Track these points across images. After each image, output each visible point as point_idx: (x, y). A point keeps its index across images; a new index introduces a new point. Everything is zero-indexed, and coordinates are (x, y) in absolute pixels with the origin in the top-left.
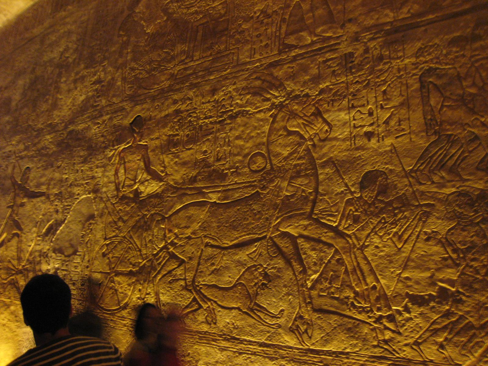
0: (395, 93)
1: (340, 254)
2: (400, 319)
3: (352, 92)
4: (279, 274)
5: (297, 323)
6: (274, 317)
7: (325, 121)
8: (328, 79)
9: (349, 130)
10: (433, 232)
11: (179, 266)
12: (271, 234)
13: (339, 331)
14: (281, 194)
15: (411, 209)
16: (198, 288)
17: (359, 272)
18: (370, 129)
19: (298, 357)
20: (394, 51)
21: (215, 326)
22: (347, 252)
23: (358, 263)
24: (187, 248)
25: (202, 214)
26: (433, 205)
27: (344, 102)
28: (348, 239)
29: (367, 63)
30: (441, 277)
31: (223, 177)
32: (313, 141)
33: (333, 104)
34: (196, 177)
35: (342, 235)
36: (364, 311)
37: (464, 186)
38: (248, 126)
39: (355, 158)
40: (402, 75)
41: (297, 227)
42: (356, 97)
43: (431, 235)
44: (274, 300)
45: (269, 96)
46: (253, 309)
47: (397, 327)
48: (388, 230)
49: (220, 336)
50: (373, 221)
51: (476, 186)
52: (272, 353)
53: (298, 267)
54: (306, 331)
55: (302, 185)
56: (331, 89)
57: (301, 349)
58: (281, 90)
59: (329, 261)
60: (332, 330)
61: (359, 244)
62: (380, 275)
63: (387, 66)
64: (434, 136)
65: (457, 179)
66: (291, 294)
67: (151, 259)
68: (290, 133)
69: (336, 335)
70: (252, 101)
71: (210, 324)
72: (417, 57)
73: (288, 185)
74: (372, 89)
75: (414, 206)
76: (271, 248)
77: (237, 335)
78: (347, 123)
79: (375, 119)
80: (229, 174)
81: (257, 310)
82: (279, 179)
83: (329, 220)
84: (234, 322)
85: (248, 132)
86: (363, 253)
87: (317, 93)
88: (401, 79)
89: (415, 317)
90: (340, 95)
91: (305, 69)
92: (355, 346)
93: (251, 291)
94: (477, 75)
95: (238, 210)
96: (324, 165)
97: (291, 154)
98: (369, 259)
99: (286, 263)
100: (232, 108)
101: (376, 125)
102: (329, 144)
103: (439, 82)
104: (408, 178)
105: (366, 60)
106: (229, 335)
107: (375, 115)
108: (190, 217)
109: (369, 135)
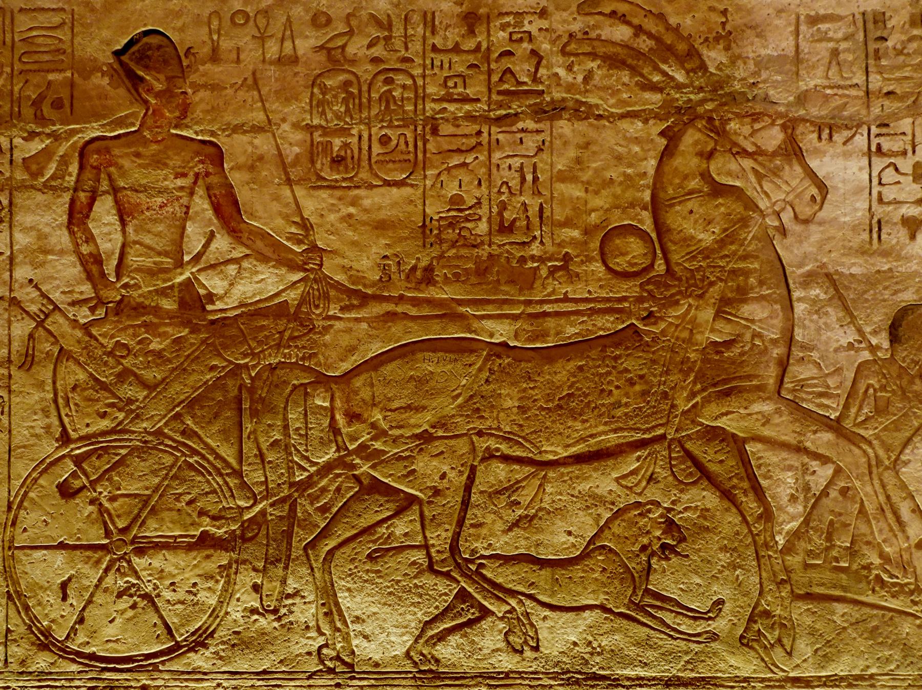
1: (849, 477)
5: (756, 627)
6: (697, 616)
11: (397, 513)
12: (677, 431)
13: (855, 635)
17: (889, 515)
23: (888, 497)
24: (420, 465)
25: (462, 376)
27: (858, 137)
28: (865, 447)
34: (429, 269)
36: (902, 591)
38: (594, 148)
39: (879, 272)
41: (743, 417)
42: (884, 130)
44: (698, 581)
45: (656, 78)
46: (643, 604)
53: (751, 505)
54: (779, 640)
55: (753, 321)
57: (769, 680)
59: (825, 493)
60: (838, 634)
66: (739, 567)
67: (290, 496)
68: (718, 190)
69: (847, 644)
70: (606, 82)
76: (681, 463)
83: (820, 406)
84: (591, 638)
85: (594, 165)
87: (791, 99)
92: (888, 660)
95: (581, 368)
96: (809, 280)
99: (721, 497)
100: (541, 88)
102: (815, 233)
106: (580, 673)
108: (420, 382)
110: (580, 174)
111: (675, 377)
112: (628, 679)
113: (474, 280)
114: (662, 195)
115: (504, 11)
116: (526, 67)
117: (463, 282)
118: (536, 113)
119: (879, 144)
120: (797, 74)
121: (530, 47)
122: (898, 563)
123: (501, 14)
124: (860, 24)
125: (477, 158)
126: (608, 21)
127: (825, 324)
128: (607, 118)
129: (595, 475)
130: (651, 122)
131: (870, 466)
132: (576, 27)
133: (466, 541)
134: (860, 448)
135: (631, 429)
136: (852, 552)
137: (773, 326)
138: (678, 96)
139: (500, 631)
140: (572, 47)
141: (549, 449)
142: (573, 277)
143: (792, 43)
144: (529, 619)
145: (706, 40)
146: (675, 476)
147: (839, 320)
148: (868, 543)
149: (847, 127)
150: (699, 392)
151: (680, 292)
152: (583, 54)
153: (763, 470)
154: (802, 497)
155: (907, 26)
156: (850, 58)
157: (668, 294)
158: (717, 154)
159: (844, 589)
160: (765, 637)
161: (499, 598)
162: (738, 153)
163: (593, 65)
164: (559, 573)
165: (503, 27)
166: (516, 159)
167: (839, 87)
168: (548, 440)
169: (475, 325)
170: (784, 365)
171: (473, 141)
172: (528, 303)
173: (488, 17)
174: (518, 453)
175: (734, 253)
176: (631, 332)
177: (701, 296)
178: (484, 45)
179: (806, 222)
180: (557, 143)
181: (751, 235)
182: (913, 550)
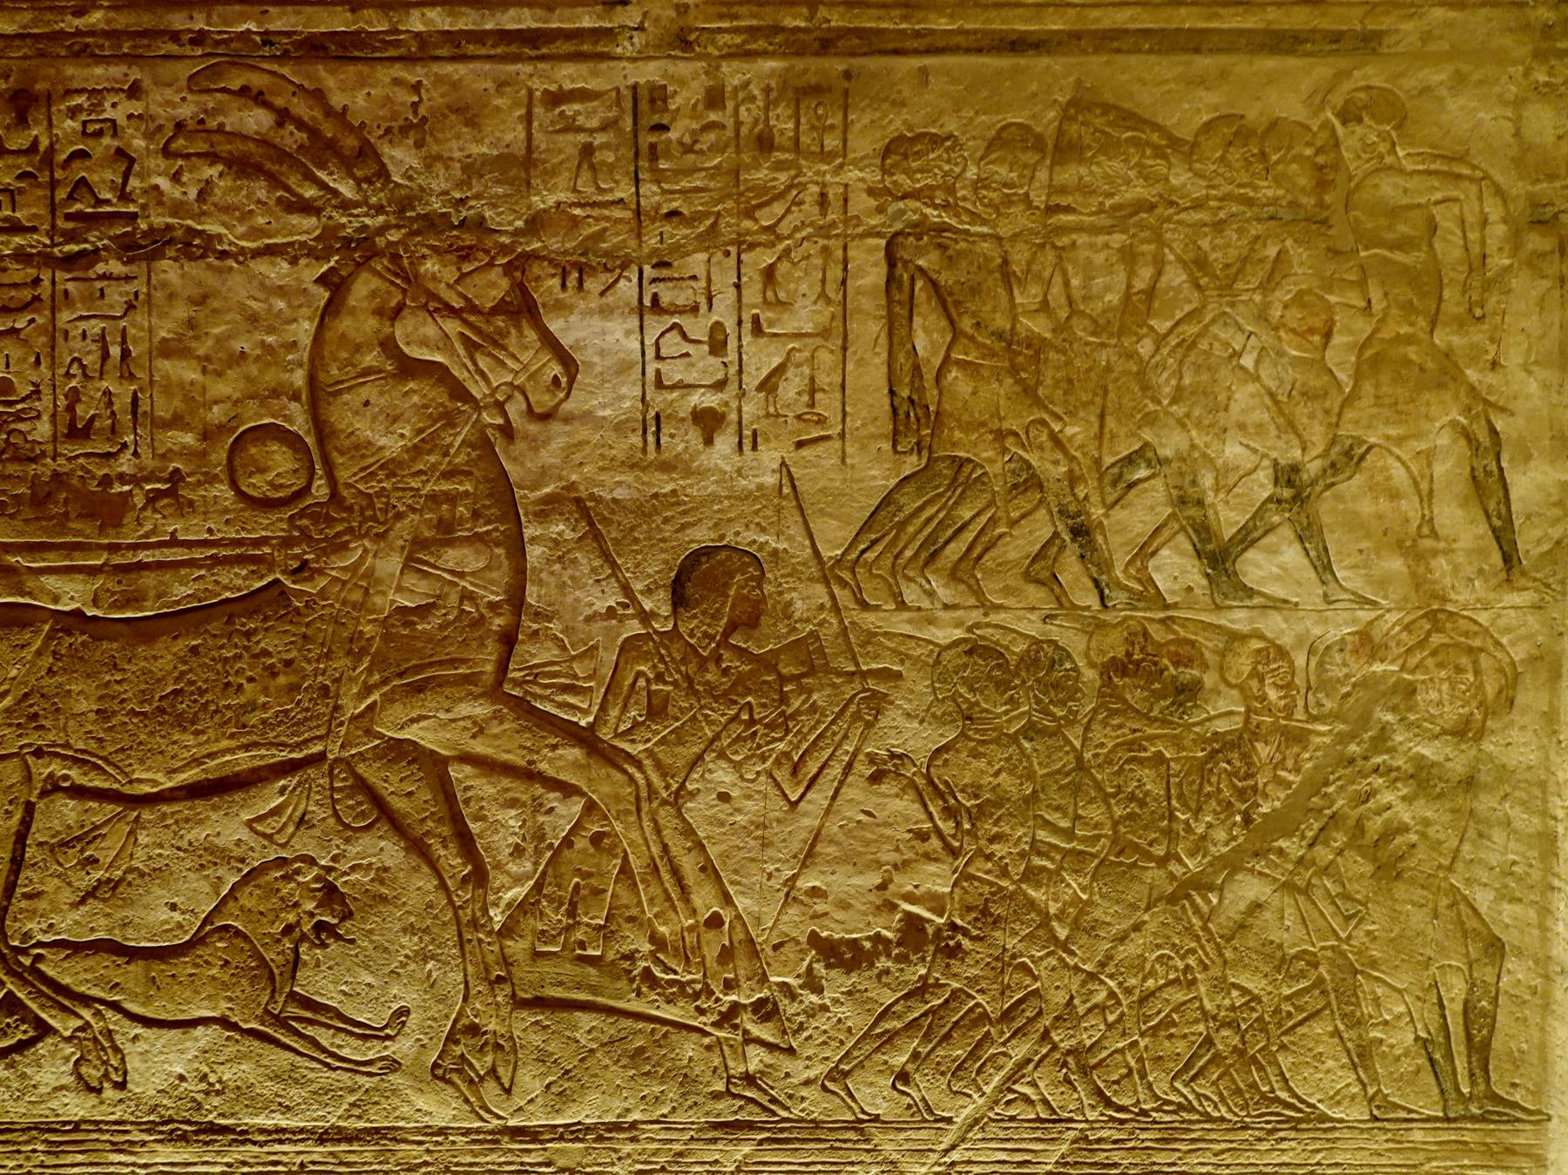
0: (804, 288)
1: (605, 817)
2: (791, 1011)
3: (654, 252)
4: (384, 891)
5: (458, 1050)
6: (368, 1034)
7: (550, 342)
8: (563, 179)
9: (638, 392)
10: (893, 756)
14: (378, 600)
15: (834, 685)
16: (27, 961)
17: (666, 876)
18: (711, 400)
19: (469, 1159)
20: (813, 128)
21: (119, 1095)
22: (627, 812)
23: (665, 848)
26: (899, 675)
27: (622, 283)
28: (631, 770)
29: (716, 148)
30: (909, 888)
31: (106, 510)
32: (505, 414)
33: (581, 281)
35: (610, 757)
37: (988, 625)
39: (656, 496)
40: (833, 224)
41: (444, 725)
42: (665, 273)
43: (890, 766)
45: (310, 192)
47: (784, 1032)
48: (759, 746)
49: (150, 1128)
50: (714, 716)
51: (1022, 627)
52: (369, 1157)
53: (453, 863)
54: (493, 1071)
55: (461, 575)
56: (575, 222)
57: (478, 1131)
58: (369, 181)
59: (567, 842)
61: (667, 787)
62: (732, 883)
63: (783, 177)
64: (914, 458)
65: (972, 601)
68: (409, 368)
71: (99, 1091)
72: (885, 171)
73: (406, 567)
74: (727, 254)
75: (839, 674)
77: (222, 1115)
78: (631, 366)
79: (733, 370)
80: (139, 501)
81: (300, 1019)
82: (366, 542)
83: (561, 705)
84: (206, 1069)
85: (216, 331)
86: (680, 815)
87: (519, 224)
88: (828, 237)
89: (836, 1001)
90: (606, 254)
91: (470, 114)
93: (269, 956)
94: (1058, 279)
95: (194, 650)
96: (547, 509)
97: (416, 451)
98: (701, 834)
99: (406, 849)
100: (132, 208)
101: (732, 388)
102: (559, 436)
103: (946, 278)
104: (828, 585)
105: (711, 136)
106: (188, 1122)
107: (732, 356)
109: (708, 422)
110: (193, 345)
111: (341, 663)
112: (262, 1131)
113: (28, 513)
114: (322, 376)
115: (75, 85)
116: (109, 175)
117: (12, 516)
118: (128, 248)
119: (655, 295)
120: (528, 183)
121: (116, 143)
122: (676, 949)
123: (69, 93)
124: (628, 105)
125: (32, 321)
126: (235, 103)
127: (572, 578)
128: (234, 256)
129: (214, 817)
130: (303, 261)
131: (638, 798)
132: (186, 111)
133: (15, 920)
135: (272, 744)
136: (606, 933)
137: (492, 582)
138: (344, 220)
139: (67, 1059)
140: (180, 143)
141: (144, 776)
142: (185, 508)
143: (522, 135)
144: (112, 1041)
145: (388, 131)
146: (339, 819)
147: (594, 570)
148: (631, 919)
149: (607, 269)
150: (376, 686)
151: (350, 530)
152: (198, 155)
153: (474, 806)
154: (530, 849)
155: (700, 107)
156: (610, 157)
157: (331, 532)
158: (405, 312)
159: (593, 989)
160: (471, 1066)
161: (64, 1009)
162: (437, 310)
163: (212, 172)
164: (157, 969)
165: (73, 112)
166: (93, 322)
167: (594, 205)
168: (142, 762)
169: (31, 583)
170: (509, 640)
171: (27, 294)
172: (114, 548)
173: (49, 97)
174: (97, 783)
175: (434, 467)
176: (275, 591)
177: (380, 537)
178: (44, 143)
179: (546, 417)
180: (158, 295)
181: (460, 439)
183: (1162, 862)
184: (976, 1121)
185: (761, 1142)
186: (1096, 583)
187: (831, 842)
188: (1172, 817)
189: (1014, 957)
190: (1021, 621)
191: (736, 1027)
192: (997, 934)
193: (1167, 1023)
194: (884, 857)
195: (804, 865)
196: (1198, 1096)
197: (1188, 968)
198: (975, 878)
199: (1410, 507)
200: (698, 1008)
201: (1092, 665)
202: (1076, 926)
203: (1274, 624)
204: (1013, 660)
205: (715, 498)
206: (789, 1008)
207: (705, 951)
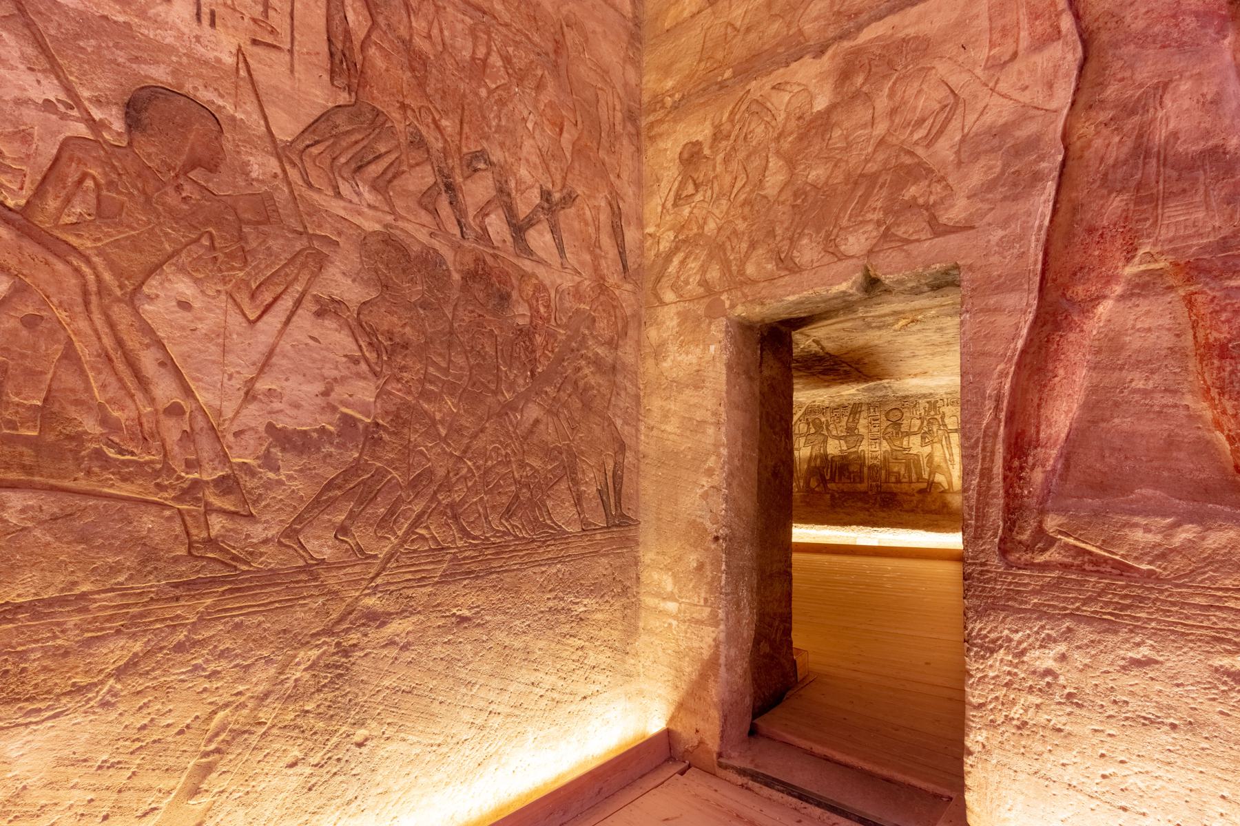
10: (333, 300)
17: (121, 367)
23: (120, 343)
39: (105, 18)
65: (387, 209)
86: (136, 312)
89: (290, 477)
98: (161, 334)
104: (281, 161)
131: (85, 293)
134: (68, 263)
182: (162, 417)
183: (495, 393)
184: (392, 555)
185: (223, 593)
186: (459, 222)
187: (284, 356)
188: (498, 368)
189: (415, 446)
190: (416, 231)
191: (198, 500)
192: (406, 431)
193: (498, 485)
194: (326, 372)
195: (261, 371)
196: (513, 526)
197: (507, 455)
198: (390, 393)
199: (591, 230)
200: (157, 485)
201: (458, 271)
202: (450, 428)
203: (541, 272)
204: (413, 255)
205: (171, 50)
206: (249, 483)
207: (166, 435)
